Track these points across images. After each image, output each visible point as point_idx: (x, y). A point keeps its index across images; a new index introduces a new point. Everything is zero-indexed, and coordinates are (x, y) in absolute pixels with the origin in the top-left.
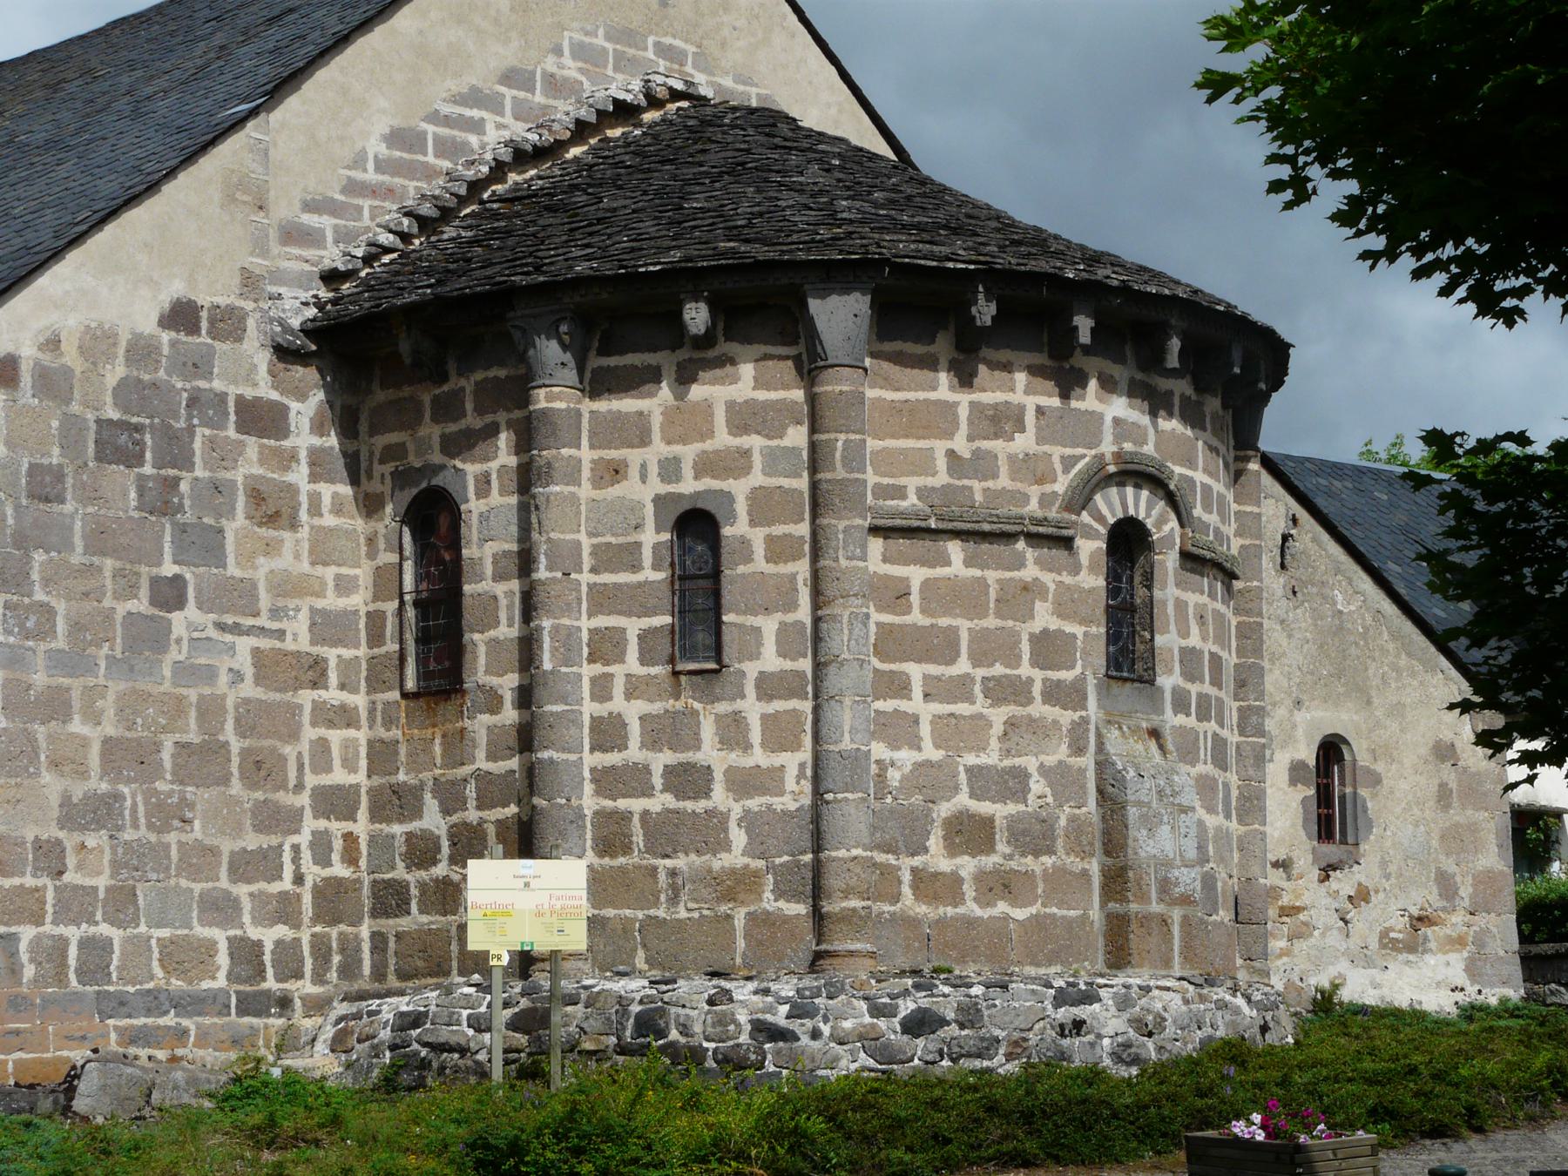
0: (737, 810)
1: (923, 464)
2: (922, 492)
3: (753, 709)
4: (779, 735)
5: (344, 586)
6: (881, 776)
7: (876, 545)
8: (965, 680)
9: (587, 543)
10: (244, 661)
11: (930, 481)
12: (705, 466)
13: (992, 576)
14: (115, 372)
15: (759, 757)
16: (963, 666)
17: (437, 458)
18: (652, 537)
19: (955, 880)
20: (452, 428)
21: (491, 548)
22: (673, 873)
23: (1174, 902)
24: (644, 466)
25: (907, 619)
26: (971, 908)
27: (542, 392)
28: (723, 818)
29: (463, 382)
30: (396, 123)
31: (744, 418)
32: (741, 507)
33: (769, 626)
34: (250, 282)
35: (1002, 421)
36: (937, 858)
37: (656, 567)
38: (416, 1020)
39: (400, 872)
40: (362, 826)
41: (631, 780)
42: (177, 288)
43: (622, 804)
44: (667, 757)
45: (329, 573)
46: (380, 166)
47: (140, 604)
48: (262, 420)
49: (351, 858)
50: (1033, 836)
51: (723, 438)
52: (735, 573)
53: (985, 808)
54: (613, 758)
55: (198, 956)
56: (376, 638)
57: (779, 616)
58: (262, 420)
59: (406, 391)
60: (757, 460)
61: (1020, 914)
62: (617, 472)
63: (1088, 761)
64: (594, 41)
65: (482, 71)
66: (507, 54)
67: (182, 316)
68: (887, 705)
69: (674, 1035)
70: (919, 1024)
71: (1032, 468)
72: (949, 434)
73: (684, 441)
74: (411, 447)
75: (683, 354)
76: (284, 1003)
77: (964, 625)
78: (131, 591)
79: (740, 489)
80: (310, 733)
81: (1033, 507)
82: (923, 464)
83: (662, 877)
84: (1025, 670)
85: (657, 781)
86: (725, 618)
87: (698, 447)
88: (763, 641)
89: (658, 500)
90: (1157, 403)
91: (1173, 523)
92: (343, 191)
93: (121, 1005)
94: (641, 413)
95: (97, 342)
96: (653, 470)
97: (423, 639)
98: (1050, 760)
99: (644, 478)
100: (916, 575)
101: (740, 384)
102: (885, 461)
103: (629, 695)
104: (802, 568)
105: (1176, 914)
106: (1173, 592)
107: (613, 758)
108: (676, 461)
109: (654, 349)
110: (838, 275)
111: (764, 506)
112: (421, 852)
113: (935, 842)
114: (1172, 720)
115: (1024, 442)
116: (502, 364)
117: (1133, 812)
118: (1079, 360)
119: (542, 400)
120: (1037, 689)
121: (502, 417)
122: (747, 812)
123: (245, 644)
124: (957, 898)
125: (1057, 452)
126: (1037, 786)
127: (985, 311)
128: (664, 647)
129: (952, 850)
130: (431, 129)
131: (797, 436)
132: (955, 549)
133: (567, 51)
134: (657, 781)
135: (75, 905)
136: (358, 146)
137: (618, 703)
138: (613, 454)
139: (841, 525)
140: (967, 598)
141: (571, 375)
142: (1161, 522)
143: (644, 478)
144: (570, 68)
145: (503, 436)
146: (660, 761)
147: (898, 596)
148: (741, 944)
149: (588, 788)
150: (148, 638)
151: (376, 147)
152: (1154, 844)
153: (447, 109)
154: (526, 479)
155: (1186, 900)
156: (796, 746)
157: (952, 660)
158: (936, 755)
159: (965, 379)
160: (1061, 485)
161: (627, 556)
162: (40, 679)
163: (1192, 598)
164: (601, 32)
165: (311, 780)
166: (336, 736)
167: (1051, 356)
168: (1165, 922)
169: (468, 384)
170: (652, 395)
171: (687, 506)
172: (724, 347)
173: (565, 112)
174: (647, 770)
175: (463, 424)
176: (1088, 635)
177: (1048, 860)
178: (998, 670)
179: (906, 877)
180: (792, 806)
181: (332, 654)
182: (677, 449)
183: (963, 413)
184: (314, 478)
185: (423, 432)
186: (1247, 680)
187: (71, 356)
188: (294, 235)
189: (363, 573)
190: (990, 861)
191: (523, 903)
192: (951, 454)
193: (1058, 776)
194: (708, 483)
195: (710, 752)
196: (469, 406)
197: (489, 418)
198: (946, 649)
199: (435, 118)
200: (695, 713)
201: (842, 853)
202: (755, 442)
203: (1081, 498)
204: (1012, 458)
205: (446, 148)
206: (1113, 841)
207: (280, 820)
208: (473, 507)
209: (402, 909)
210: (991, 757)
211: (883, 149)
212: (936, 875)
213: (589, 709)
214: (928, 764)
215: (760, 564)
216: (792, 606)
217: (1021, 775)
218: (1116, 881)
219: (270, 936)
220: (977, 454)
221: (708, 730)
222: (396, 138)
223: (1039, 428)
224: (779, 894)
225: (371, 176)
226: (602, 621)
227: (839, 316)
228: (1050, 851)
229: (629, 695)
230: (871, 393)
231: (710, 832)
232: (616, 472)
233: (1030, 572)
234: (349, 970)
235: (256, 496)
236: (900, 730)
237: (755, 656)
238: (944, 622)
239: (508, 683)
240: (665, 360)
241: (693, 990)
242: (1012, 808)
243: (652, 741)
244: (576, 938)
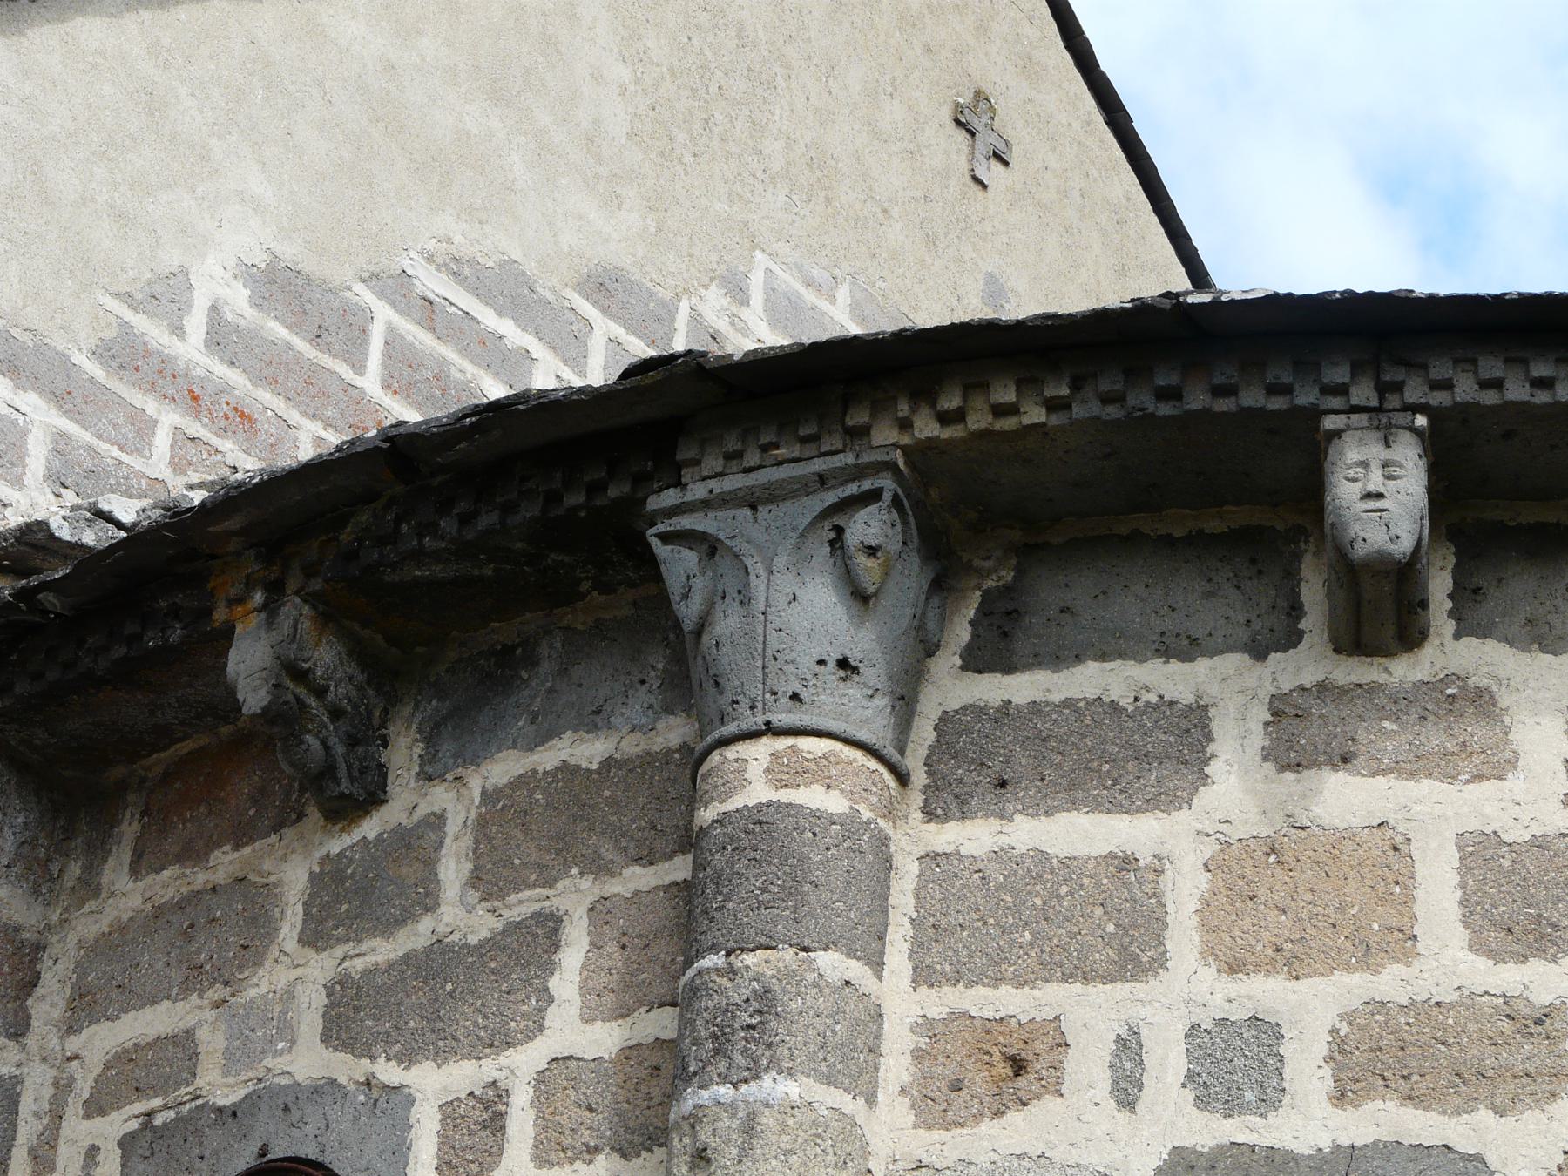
17: (308, 1060)
20: (381, 951)
24: (1129, 1047)
27: (758, 753)
29: (441, 797)
30: (289, 251)
51: (1448, 962)
59: (225, 863)
62: (1018, 1066)
64: (824, 305)
73: (1290, 961)
74: (212, 1041)
75: (1308, 664)
92: (104, 353)
94: (1126, 862)
96: (1168, 1061)
99: (1127, 1090)
101: (1515, 784)
108: (1264, 1033)
109: (1185, 648)
116: (594, 720)
119: (751, 777)
121: (574, 897)
130: (383, 314)
133: (757, 298)
136: (171, 258)
141: (869, 714)
143: (1127, 1090)
145: (573, 955)
151: (218, 285)
153: (433, 283)
164: (843, 293)
169: (456, 804)
170: (1165, 801)
175: (418, 935)
182: (1266, 992)
185: (263, 983)
196: (452, 871)
197: (523, 905)
199: (397, 288)
222: (277, 284)
240: (1230, 688)
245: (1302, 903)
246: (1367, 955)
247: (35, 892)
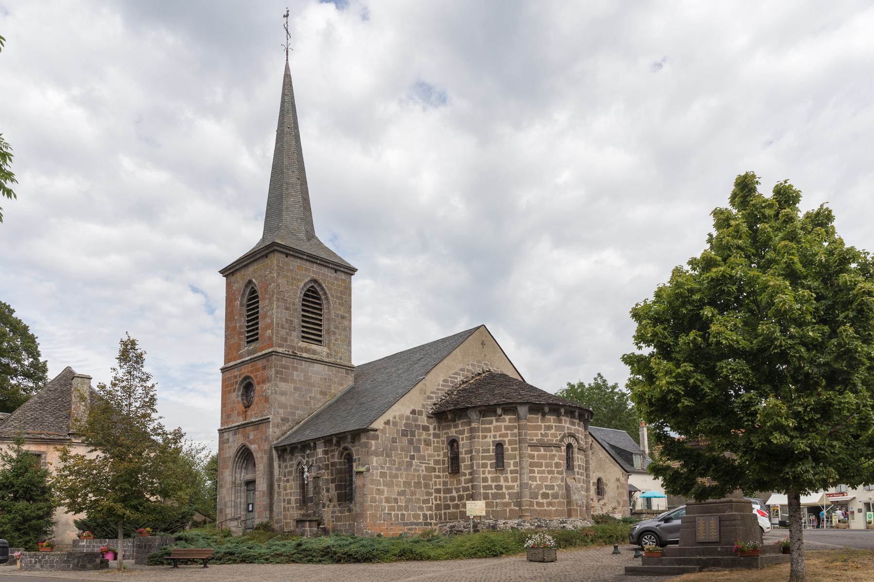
1: (537, 435)
3: (509, 476)
4: (514, 480)
5: (439, 455)
7: (529, 448)
10: (424, 468)
12: (500, 436)
14: (404, 422)
15: (510, 484)
18: (492, 448)
21: (464, 450)
31: (507, 428)
33: (512, 462)
34: (423, 406)
35: (549, 428)
36: (540, 500)
38: (454, 527)
39: (449, 502)
40: (442, 495)
41: (489, 487)
42: (413, 408)
47: (408, 459)
48: (426, 429)
49: (440, 500)
50: (555, 496)
51: (504, 431)
52: (506, 453)
55: (416, 516)
56: (444, 464)
58: (426, 429)
63: (563, 483)
65: (457, 370)
66: (461, 366)
67: (413, 412)
71: (554, 435)
76: (431, 524)
78: (406, 457)
79: (506, 440)
82: (537, 435)
90: (573, 424)
93: (406, 524)
95: (401, 417)
97: (452, 464)
100: (536, 453)
102: (530, 435)
104: (517, 453)
110: (521, 404)
112: (453, 499)
113: (540, 497)
114: (577, 476)
115: (553, 431)
123: (424, 465)
127: (547, 409)
129: (542, 498)
131: (516, 431)
132: (542, 449)
135: (400, 508)
137: (486, 475)
140: (544, 457)
144: (470, 368)
146: (494, 484)
147: (532, 457)
150: (410, 464)
151: (441, 383)
152: (575, 497)
154: (471, 438)
159: (543, 420)
161: (488, 451)
162: (394, 472)
169: (460, 422)
172: (503, 416)
173: (470, 375)
176: (563, 462)
181: (437, 467)
187: (397, 420)
188: (429, 398)
189: (442, 453)
191: (476, 508)
193: (559, 486)
195: (502, 483)
202: (509, 432)
203: (562, 440)
205: (452, 382)
206: (568, 496)
207: (430, 494)
208: (461, 443)
209: (449, 508)
210: (548, 483)
213: (482, 476)
215: (510, 452)
217: (553, 486)
218: (569, 503)
219: (428, 513)
221: (502, 479)
222: (444, 381)
227: (523, 410)
231: (502, 496)
232: (486, 437)
233: (554, 452)
234: (440, 518)
235: (425, 441)
236: (533, 479)
239: (467, 472)
240: (494, 418)
241: (501, 522)
243: (492, 481)
244: (484, 514)
245: (498, 429)
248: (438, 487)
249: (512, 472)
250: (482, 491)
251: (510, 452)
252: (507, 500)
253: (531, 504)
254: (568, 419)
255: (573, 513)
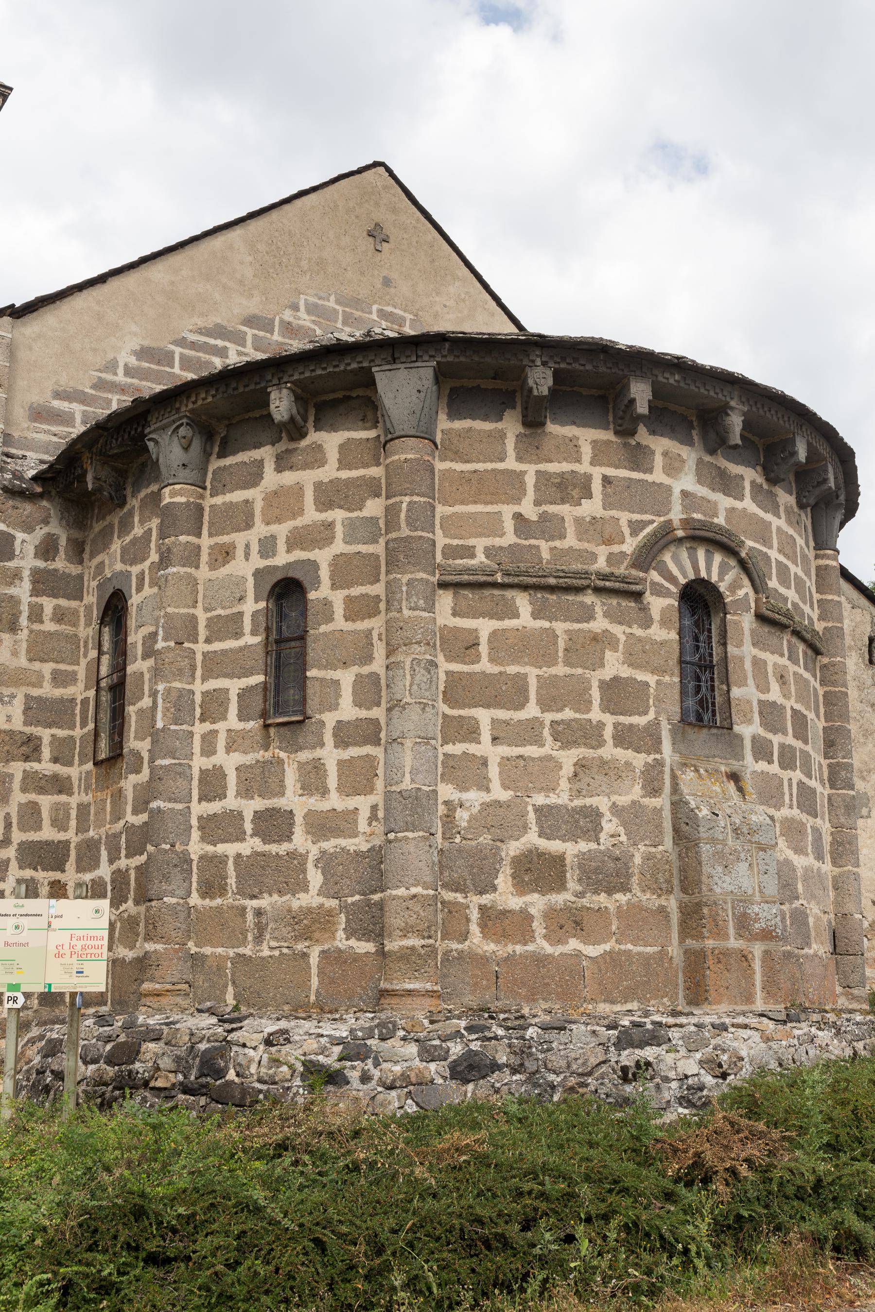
0: (314, 851)
2: (489, 552)
3: (331, 755)
6: (449, 819)
7: (445, 600)
8: (534, 724)
9: (202, 617)
11: (498, 542)
12: (296, 541)
13: (560, 627)
15: (335, 801)
16: (532, 710)
19: (525, 917)
22: (259, 913)
23: (754, 938)
24: (247, 546)
25: (476, 668)
26: (542, 945)
28: (304, 857)
30: (146, 343)
31: (329, 494)
32: (324, 573)
33: (346, 678)
35: (570, 488)
36: (506, 895)
37: (254, 633)
43: (221, 848)
44: (258, 804)
45: (47, 668)
46: (129, 371)
50: (608, 875)
51: (311, 515)
53: (555, 846)
54: (214, 807)
57: (355, 669)
60: (339, 530)
61: (593, 951)
62: (228, 553)
63: (662, 802)
64: (326, 303)
66: (253, 306)
68: (456, 749)
69: (231, 1075)
70: (469, 1069)
72: (518, 500)
73: (279, 520)
75: (282, 446)
77: (532, 673)
79: (323, 557)
80: (18, 797)
81: (601, 564)
82: (493, 526)
83: (250, 916)
84: (596, 714)
85: (248, 827)
86: (308, 674)
87: (290, 524)
88: (338, 693)
89: (258, 573)
90: (727, 485)
91: (746, 589)
92: (94, 387)
94: (247, 502)
96: (255, 548)
98: (623, 800)
100: (485, 627)
101: (327, 467)
102: (450, 524)
103: (229, 749)
105: (758, 950)
106: (744, 643)
107: (214, 807)
109: (258, 446)
111: (345, 571)
113: (504, 880)
114: (751, 766)
115: (592, 507)
117: (706, 849)
118: (643, 435)
120: (608, 733)
122: (323, 853)
124: (527, 936)
125: (624, 517)
126: (610, 825)
128: (257, 702)
129: (521, 886)
130: (178, 350)
132: (523, 602)
133: (302, 308)
134: (248, 827)
136: (110, 356)
138: (225, 539)
139: (405, 579)
140: (538, 648)
142: (735, 586)
144: (305, 319)
146: (251, 807)
147: (465, 646)
148: (315, 982)
149: (195, 834)
151: (126, 358)
152: (732, 881)
155: (767, 935)
156: (369, 789)
157: (520, 706)
158: (504, 796)
160: (630, 545)
161: (228, 626)
163: (771, 659)
164: (332, 298)
165: (17, 836)
166: (46, 802)
167: (617, 433)
168: (745, 957)
171: (279, 576)
172: (314, 437)
174: (240, 815)
176: (662, 685)
177: (622, 898)
178: (568, 714)
179: (475, 915)
180: (365, 847)
181: (46, 734)
182: (274, 528)
183: (530, 480)
184: (35, 592)
186: (834, 741)
190: (559, 899)
192: (518, 517)
193: (630, 815)
194: (299, 555)
195: (293, 800)
198: (516, 694)
199: (182, 342)
200: (281, 762)
201: (401, 892)
202: (338, 515)
204: (578, 521)
206: (689, 878)
210: (562, 797)
211: (511, 329)
212: (505, 913)
213: (199, 763)
214: (497, 803)
215: (339, 622)
216: (368, 658)
217: (594, 815)
218: (693, 918)
220: (544, 517)
222: (143, 353)
223: (605, 495)
224: (351, 933)
225: (120, 377)
226: (213, 684)
228: (625, 888)
229: (229, 749)
230: (440, 466)
231: (288, 874)
232: (225, 554)
233: (600, 624)
237: (334, 706)
238: (512, 669)
240: (266, 454)
242: (584, 846)
244: (96, 979)
245: (284, 504)
246: (294, 517)
247: (80, 529)
248: (48, 833)
249: (345, 735)
250: (196, 847)
251: (339, 622)
252: (310, 898)
253: (454, 922)
254: (690, 455)
255: (712, 975)
